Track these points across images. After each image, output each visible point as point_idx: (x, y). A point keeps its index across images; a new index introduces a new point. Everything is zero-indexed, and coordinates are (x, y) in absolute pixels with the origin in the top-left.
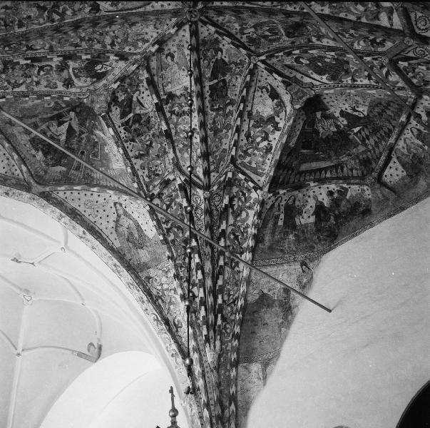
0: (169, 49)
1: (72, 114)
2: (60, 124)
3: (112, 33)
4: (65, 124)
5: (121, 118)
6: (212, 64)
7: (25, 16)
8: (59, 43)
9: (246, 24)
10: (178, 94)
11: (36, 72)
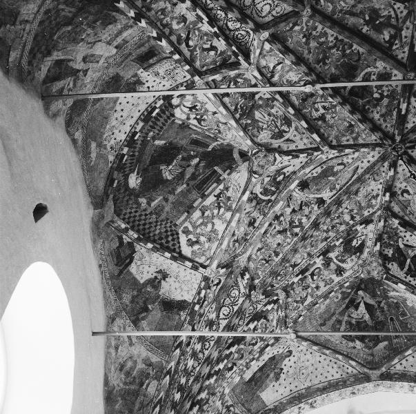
1: (360, 293)
2: (357, 308)
3: (346, 211)
4: (361, 305)
5: (402, 269)
7: (276, 246)
8: (312, 246)
11: (311, 280)
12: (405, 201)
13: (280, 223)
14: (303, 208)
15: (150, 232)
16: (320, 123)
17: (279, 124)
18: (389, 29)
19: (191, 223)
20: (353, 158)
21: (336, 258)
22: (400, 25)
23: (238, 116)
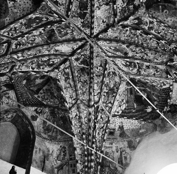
0: (104, 24)
3: (125, 36)
6: (86, 18)
7: (153, 55)
8: (147, 40)
9: (71, 35)
10: (103, 6)
11: (161, 33)
12: (107, 19)
13: (144, 56)
14: (134, 51)
15: (165, 98)
16: (103, 65)
17: (111, 76)
18: (65, 71)
19: (158, 85)
20: (106, 47)
21: (147, 26)
22: (62, 70)
23: (115, 94)
